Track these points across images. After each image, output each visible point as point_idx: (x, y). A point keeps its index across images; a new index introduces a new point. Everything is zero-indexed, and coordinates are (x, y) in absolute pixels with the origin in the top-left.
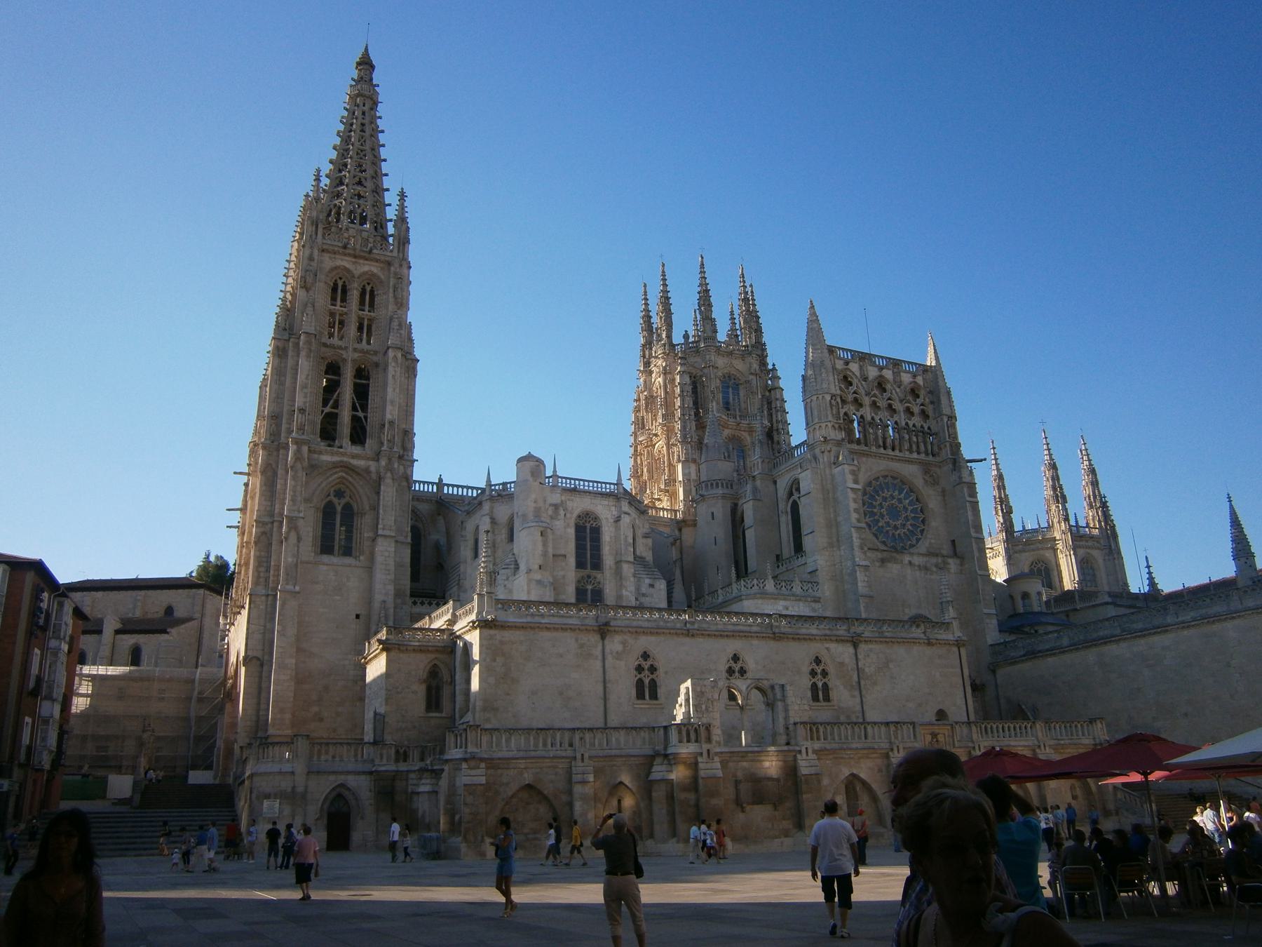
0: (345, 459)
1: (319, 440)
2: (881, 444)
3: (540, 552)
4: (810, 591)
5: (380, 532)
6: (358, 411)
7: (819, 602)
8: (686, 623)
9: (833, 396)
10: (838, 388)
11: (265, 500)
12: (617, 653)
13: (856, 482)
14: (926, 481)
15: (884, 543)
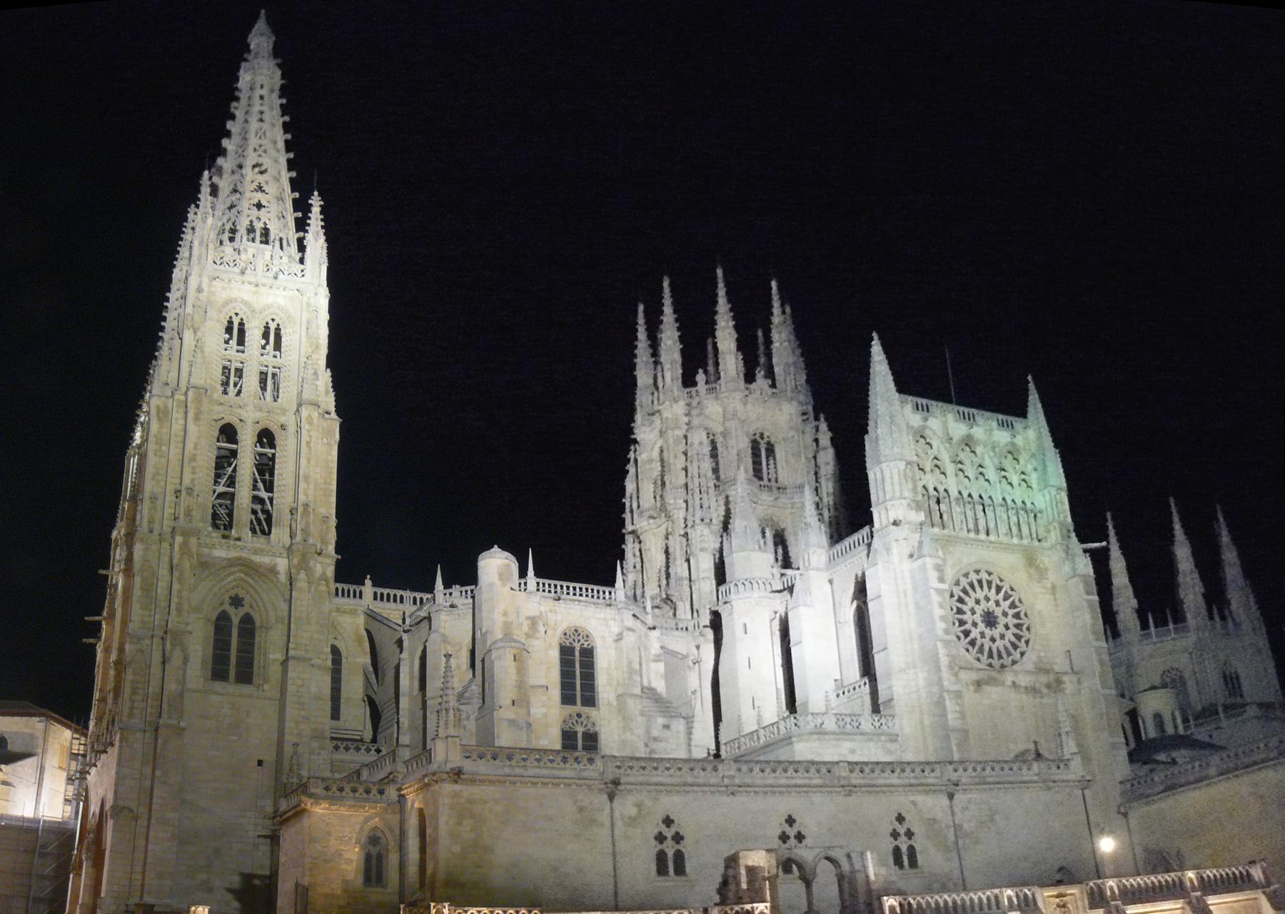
0: (244, 555)
1: (210, 529)
2: (971, 526)
3: (514, 683)
4: (884, 727)
5: (291, 653)
6: (259, 490)
7: (896, 741)
8: (723, 778)
9: (909, 463)
10: (914, 453)
11: (141, 608)
12: (630, 817)
13: (941, 580)
14: (1030, 577)
15: (978, 660)
